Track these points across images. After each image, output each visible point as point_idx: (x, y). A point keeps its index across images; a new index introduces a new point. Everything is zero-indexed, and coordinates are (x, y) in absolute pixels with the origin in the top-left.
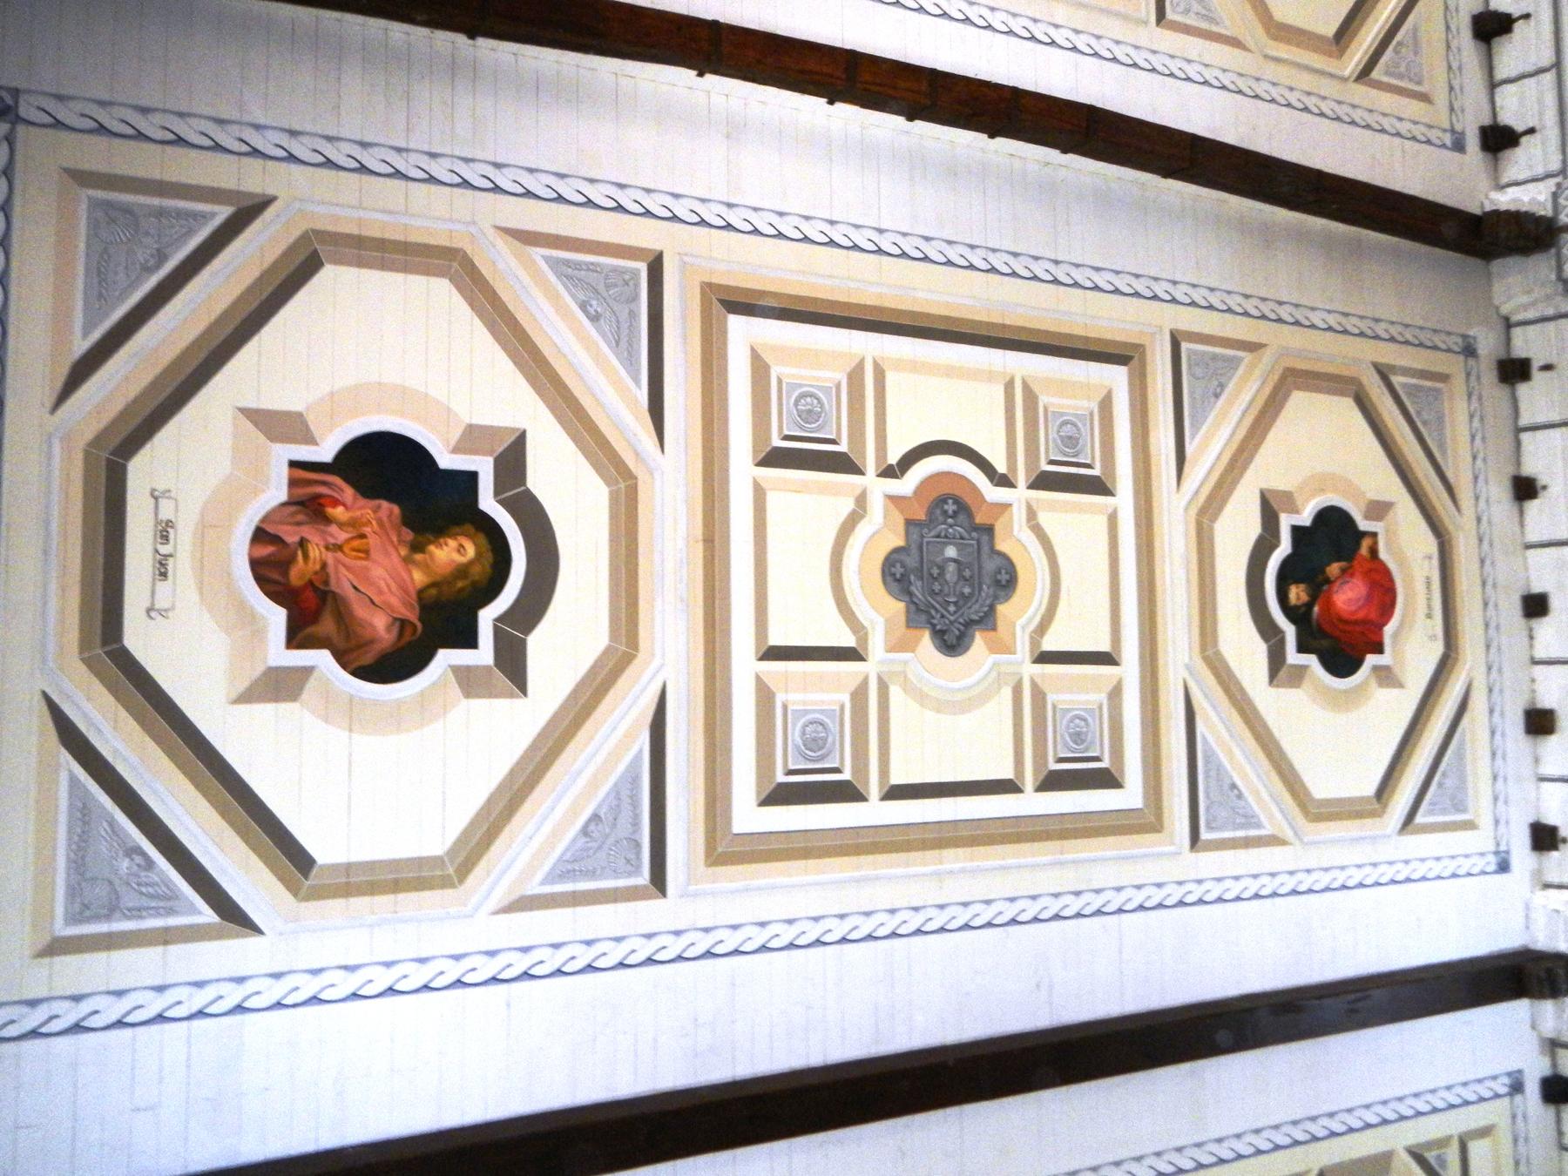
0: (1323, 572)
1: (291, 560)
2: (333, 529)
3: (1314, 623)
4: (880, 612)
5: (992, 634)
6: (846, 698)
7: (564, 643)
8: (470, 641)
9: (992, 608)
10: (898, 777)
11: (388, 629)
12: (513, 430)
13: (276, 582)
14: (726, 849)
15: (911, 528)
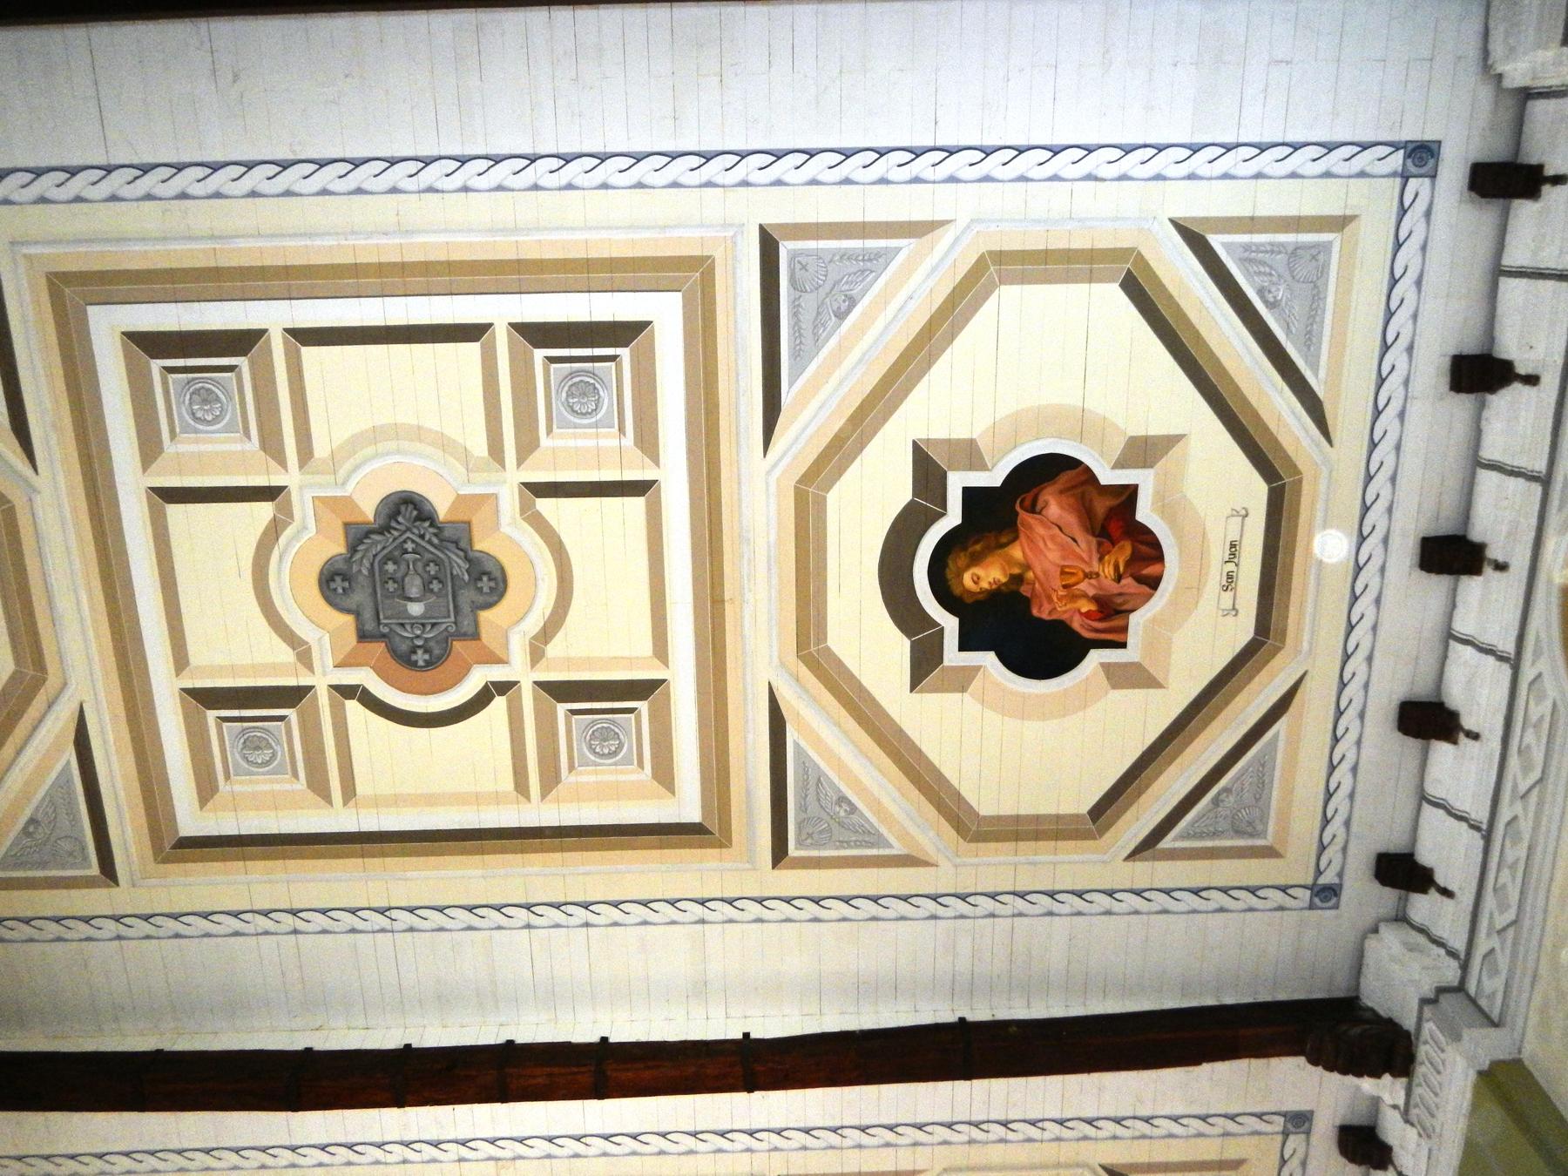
1: (1128, 564)
2: (1091, 592)
4: (506, 536)
5: (348, 519)
6: (544, 441)
7: (875, 491)
8: (969, 494)
9: (353, 549)
10: (472, 350)
11: (1046, 504)
12: (921, 691)
13: (1142, 543)
14: (691, 275)
15: (471, 630)
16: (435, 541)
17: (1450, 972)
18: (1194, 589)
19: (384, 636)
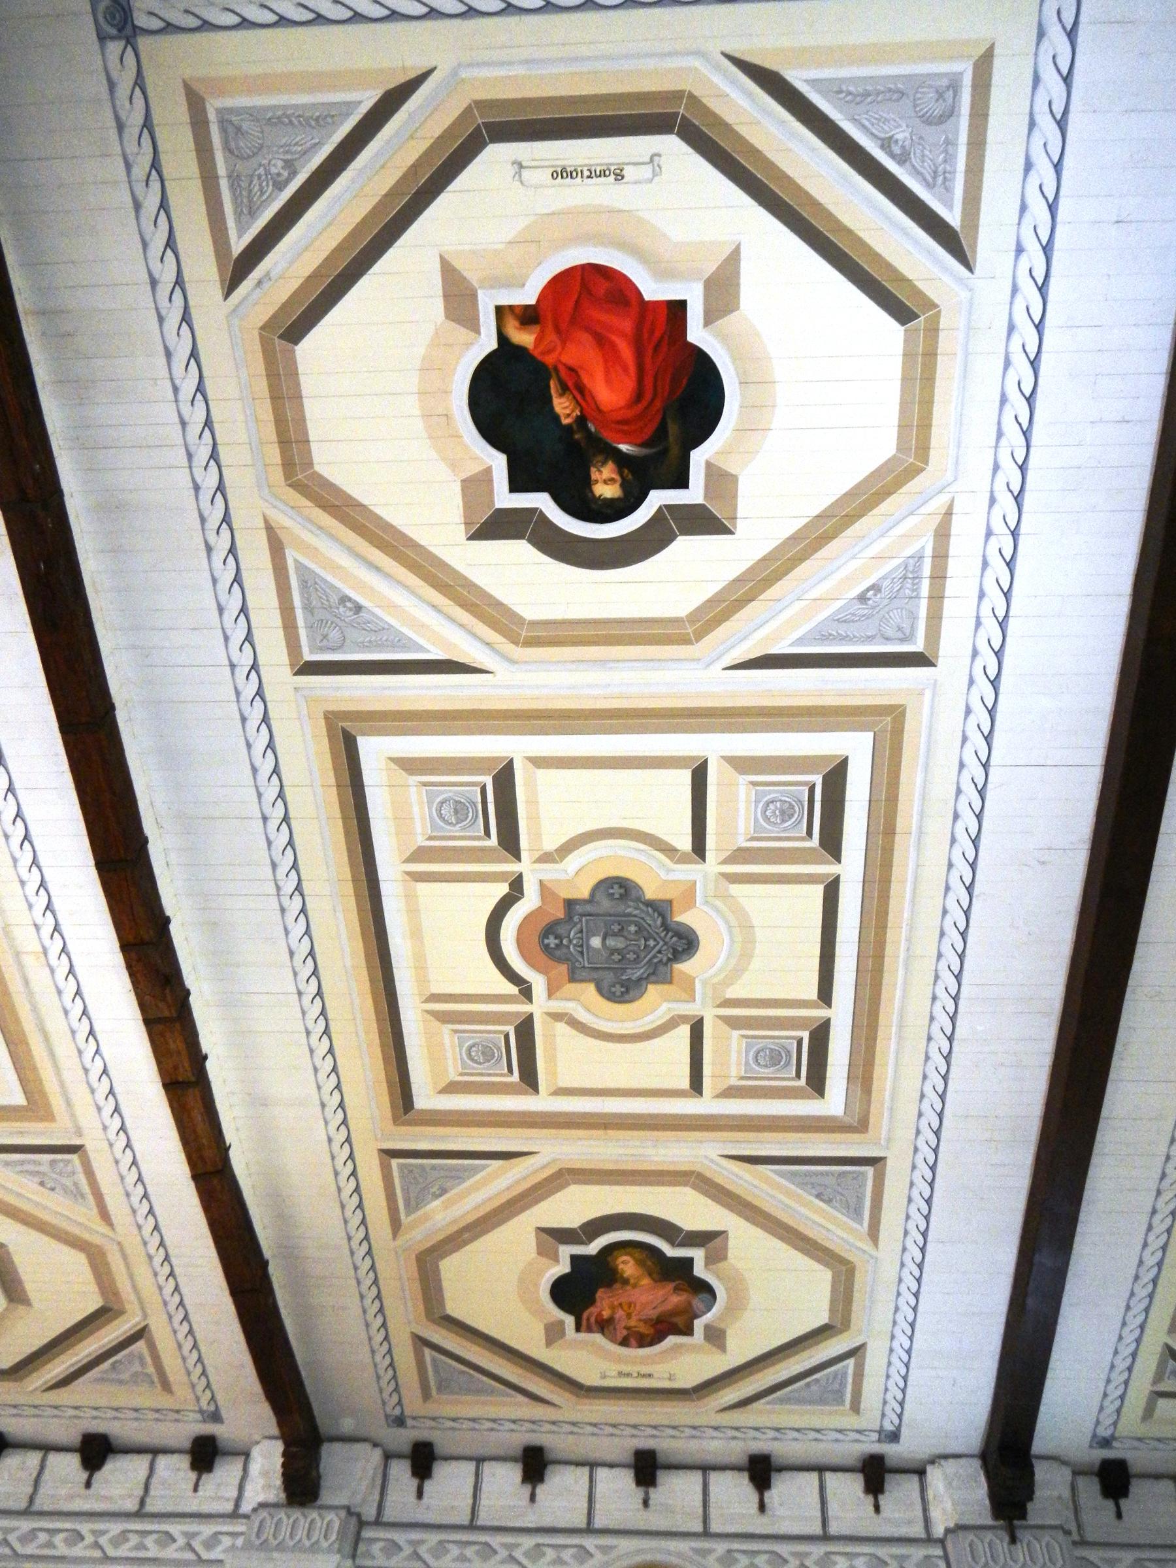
0: (569, 428)
2: (617, 1316)
3: (645, 451)
4: (656, 1004)
9: (650, 904)
10: (813, 994)
16: (655, 960)
17: (370, 1513)
18: (620, 1360)
19: (571, 918)
